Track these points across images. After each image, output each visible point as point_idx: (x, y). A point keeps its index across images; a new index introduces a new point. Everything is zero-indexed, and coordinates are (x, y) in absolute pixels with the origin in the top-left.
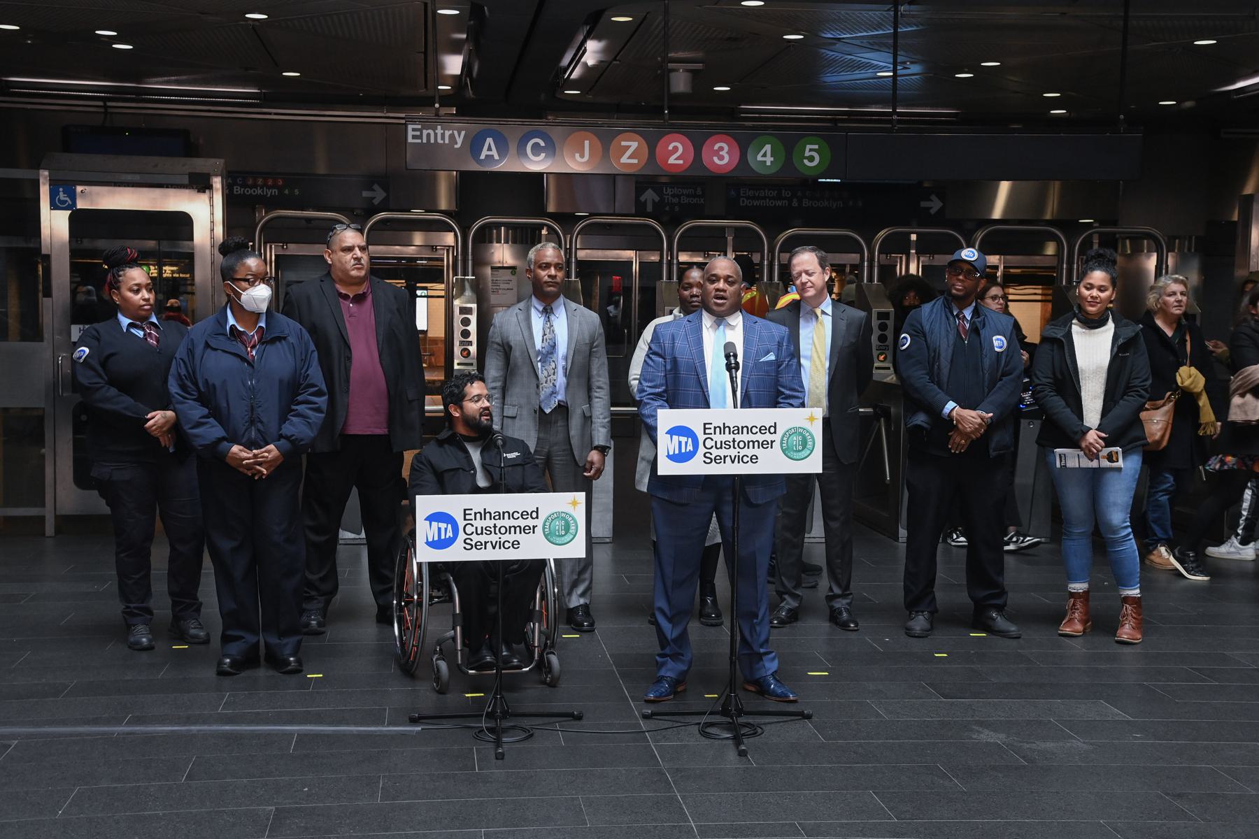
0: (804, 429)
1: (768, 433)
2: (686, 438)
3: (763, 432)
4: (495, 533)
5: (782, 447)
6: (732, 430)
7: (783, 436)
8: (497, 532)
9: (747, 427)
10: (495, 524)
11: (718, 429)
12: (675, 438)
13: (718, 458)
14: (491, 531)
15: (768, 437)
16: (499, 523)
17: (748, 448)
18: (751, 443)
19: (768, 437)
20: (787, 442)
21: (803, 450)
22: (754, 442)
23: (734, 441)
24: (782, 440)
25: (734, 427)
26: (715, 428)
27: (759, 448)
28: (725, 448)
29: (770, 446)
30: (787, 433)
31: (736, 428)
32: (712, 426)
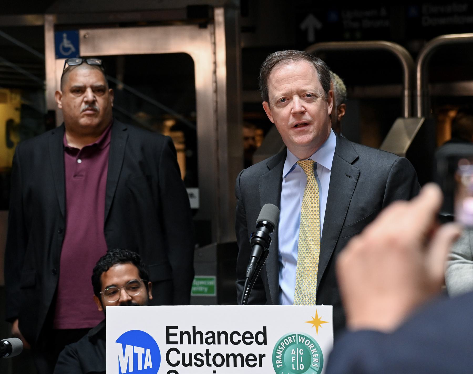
0: (307, 338)
1: (255, 342)
2: (143, 349)
3: (248, 341)
4: (209, 365)
5: (275, 365)
6: (205, 337)
7: (276, 349)
8: (211, 362)
9: (225, 333)
10: (208, 351)
11: (185, 336)
12: (129, 348)
13: (251, 358)
14: (202, 361)
15: (255, 349)
16: (214, 349)
17: (228, 365)
18: (231, 358)
19: (255, 349)
20: (282, 357)
21: (305, 370)
22: (235, 357)
23: (208, 354)
24: (275, 354)
25: (207, 334)
26: (182, 334)
27: (242, 365)
28: (196, 364)
29: (258, 362)
30: (282, 344)
31: (210, 335)
32: (177, 331)
